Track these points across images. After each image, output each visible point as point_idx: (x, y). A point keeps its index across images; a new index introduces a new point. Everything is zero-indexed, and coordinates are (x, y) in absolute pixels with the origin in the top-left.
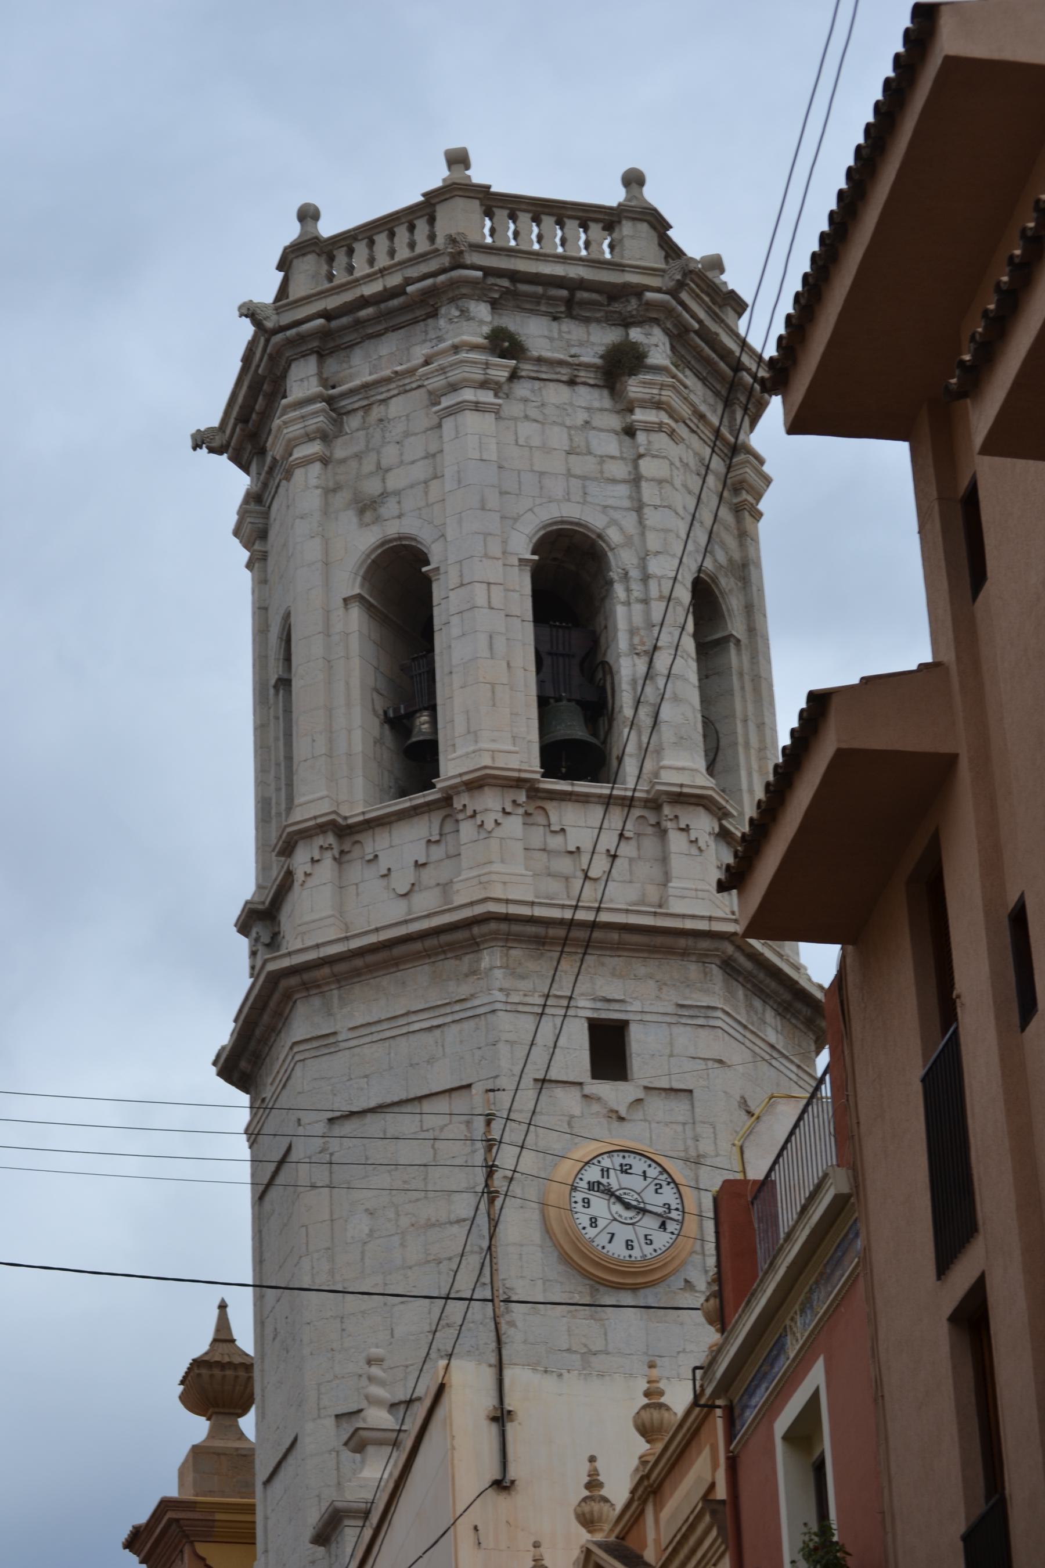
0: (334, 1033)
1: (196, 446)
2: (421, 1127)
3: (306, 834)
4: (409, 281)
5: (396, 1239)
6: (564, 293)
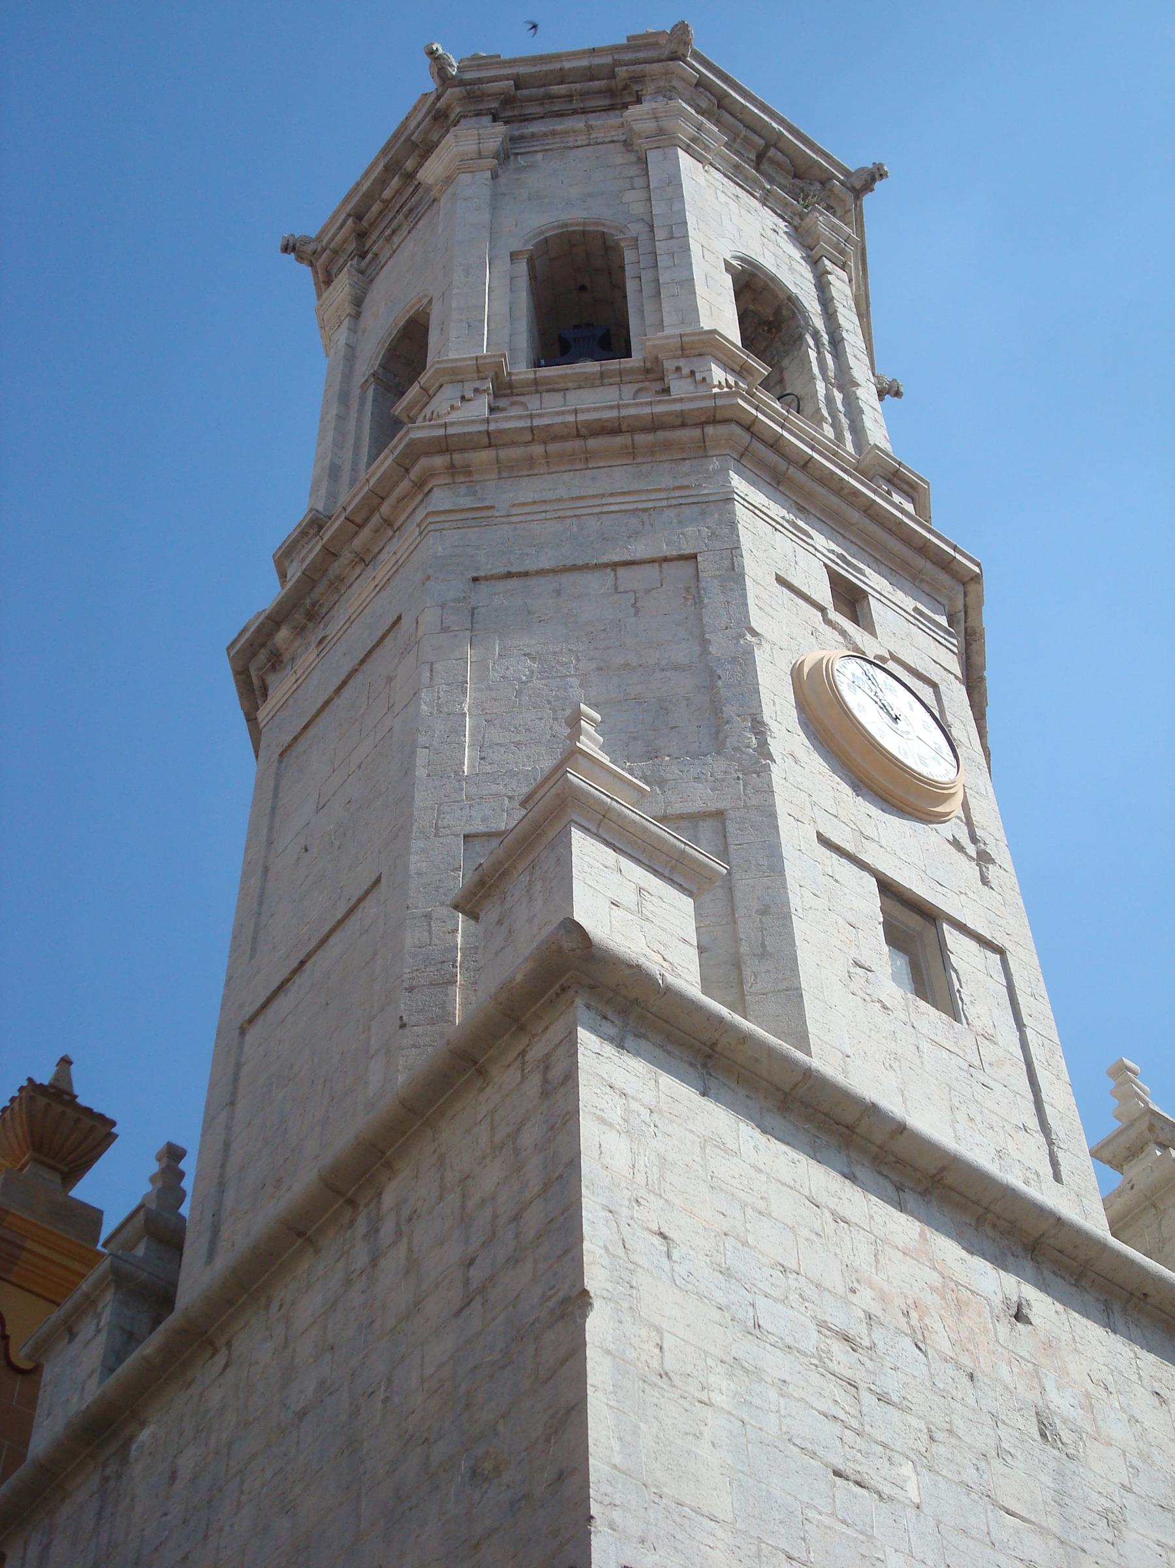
0: (492, 507)
1: (286, 249)
2: (616, 588)
3: (455, 375)
4: (617, 63)
5: (575, 681)
6: (762, 142)
